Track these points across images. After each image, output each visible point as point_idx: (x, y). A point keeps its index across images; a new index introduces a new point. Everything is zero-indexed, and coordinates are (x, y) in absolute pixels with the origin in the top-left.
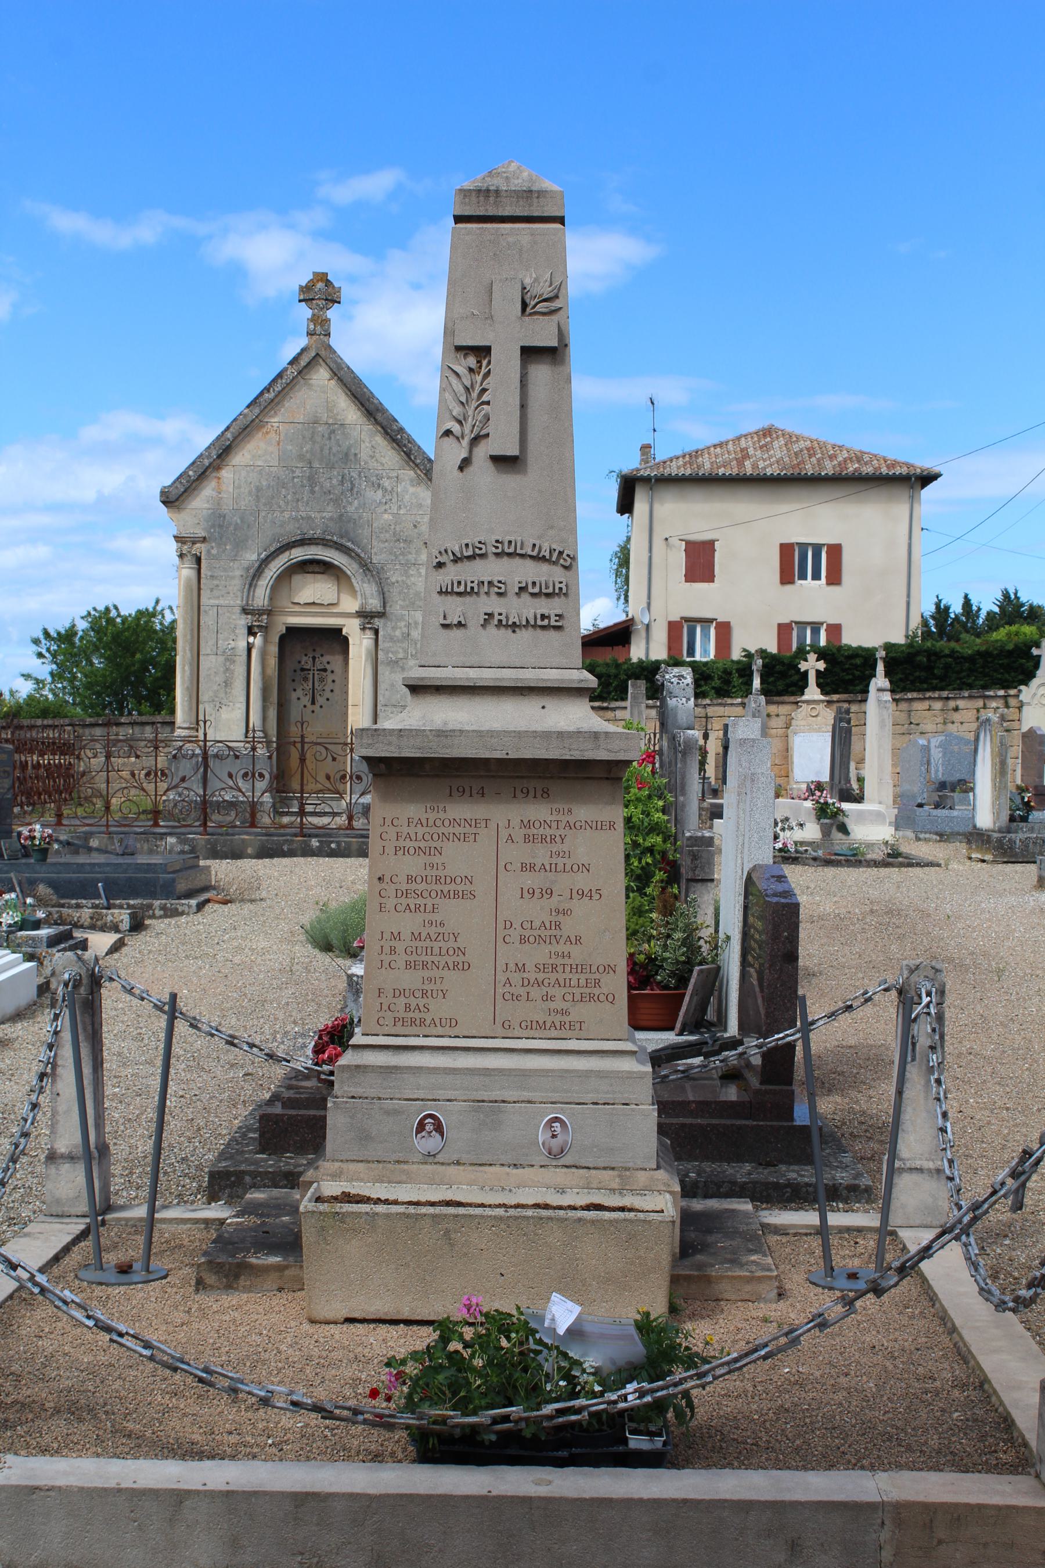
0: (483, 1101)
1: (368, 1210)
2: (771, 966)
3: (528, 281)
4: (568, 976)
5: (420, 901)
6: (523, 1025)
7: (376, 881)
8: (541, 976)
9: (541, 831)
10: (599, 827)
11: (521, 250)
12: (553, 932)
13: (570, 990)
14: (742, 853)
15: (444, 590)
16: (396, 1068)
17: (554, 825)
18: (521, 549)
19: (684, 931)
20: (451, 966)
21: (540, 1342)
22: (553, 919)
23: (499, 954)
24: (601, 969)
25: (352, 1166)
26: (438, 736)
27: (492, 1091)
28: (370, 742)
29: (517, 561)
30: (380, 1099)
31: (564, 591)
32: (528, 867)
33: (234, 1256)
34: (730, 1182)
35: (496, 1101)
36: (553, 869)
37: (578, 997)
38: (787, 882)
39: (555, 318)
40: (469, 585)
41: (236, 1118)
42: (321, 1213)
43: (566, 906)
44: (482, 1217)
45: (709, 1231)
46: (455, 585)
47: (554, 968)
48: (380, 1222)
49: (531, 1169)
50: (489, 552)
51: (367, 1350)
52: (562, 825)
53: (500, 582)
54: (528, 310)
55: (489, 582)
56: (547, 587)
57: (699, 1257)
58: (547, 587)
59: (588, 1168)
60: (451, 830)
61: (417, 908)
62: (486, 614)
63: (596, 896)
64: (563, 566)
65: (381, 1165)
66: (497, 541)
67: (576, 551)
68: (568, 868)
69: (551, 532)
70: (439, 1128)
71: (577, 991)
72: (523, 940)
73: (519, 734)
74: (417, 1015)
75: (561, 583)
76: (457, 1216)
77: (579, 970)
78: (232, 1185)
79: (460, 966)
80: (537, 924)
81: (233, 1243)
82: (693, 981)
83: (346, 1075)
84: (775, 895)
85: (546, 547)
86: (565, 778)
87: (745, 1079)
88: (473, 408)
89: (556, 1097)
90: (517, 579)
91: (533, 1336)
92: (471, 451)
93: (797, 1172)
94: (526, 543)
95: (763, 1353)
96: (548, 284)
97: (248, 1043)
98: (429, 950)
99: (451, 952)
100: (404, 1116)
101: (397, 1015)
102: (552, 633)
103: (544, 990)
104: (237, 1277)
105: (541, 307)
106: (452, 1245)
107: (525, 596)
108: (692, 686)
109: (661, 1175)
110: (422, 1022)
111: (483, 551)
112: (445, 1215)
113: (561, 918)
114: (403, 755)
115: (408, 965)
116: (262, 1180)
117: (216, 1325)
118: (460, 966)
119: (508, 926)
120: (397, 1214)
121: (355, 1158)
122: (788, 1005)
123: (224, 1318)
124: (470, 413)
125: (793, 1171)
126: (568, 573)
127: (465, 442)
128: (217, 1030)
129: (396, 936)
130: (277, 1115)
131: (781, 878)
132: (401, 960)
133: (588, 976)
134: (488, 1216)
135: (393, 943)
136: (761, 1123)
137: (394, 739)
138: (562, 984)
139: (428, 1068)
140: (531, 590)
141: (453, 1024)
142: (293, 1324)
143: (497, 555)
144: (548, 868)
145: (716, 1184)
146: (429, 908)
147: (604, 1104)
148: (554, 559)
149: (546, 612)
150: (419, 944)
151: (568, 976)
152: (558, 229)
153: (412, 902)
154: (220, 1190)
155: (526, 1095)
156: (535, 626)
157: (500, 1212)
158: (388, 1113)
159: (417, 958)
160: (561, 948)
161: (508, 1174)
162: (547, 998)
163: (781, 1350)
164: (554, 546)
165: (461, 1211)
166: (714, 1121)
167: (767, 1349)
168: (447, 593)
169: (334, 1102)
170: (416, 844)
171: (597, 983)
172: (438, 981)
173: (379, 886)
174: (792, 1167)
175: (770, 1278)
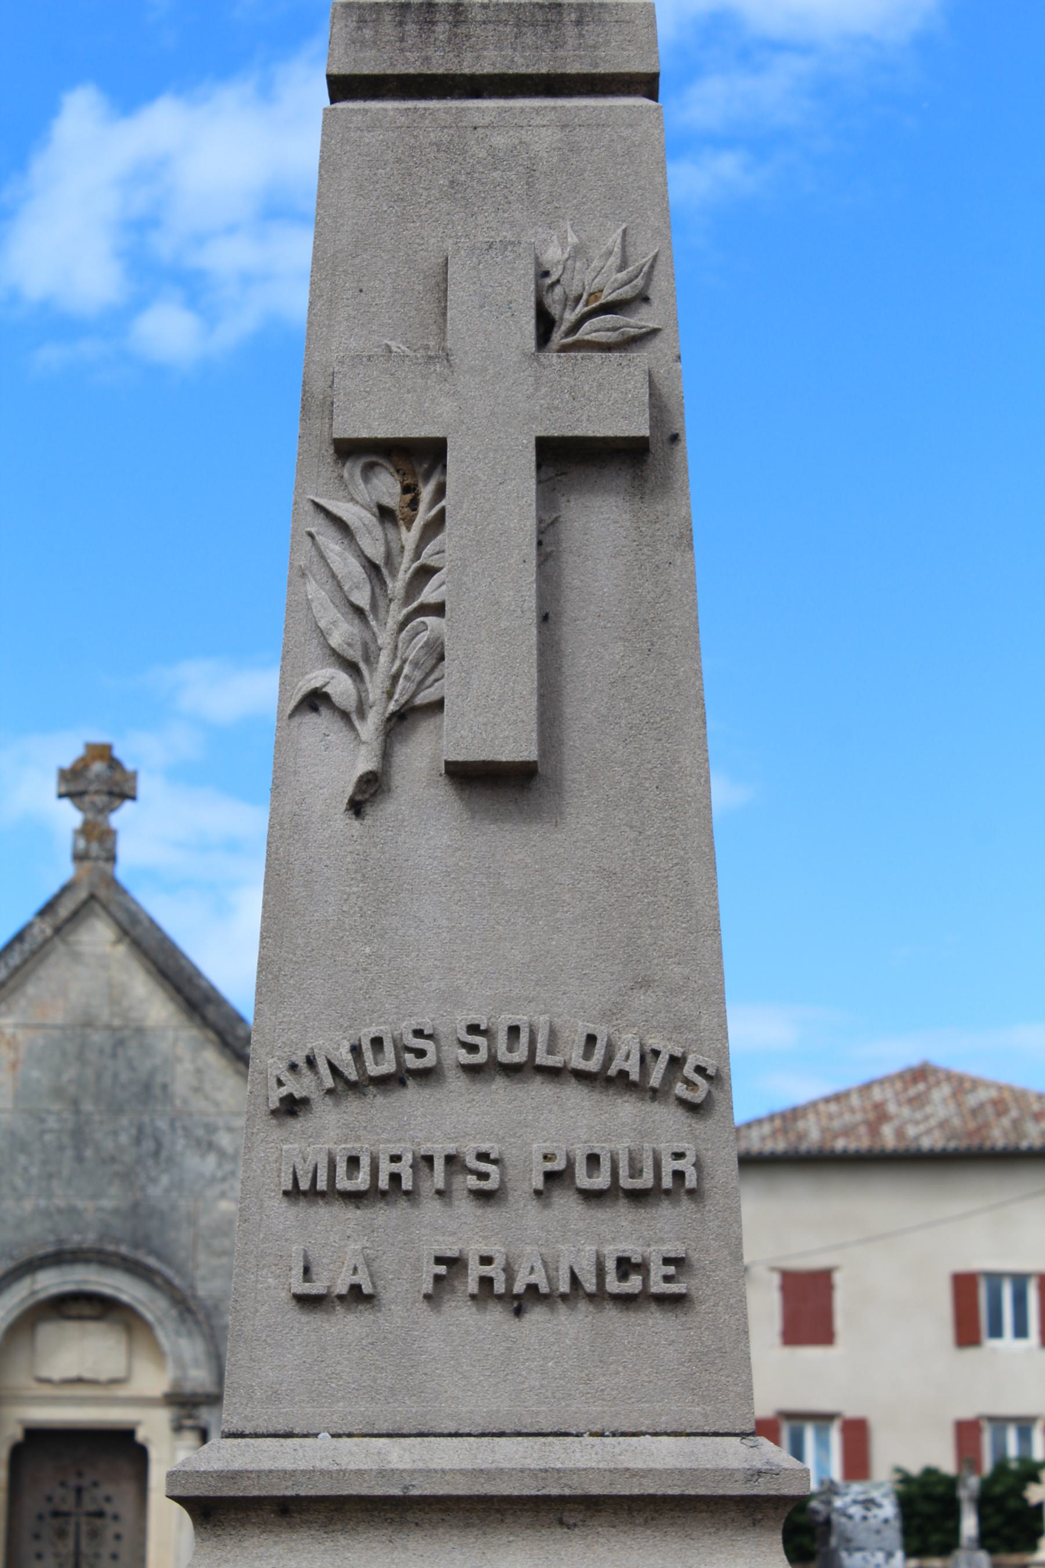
3: (553, 255)
11: (531, 170)
15: (304, 1185)
18: (550, 1051)
29: (539, 1090)
31: (691, 1182)
39: (641, 358)
40: (386, 1168)
46: (341, 1168)
50: (448, 1062)
53: (483, 1157)
54: (557, 338)
55: (451, 1160)
56: (635, 1172)
58: (635, 1172)
62: (439, 1260)
64: (683, 1102)
66: (474, 1029)
67: (723, 1053)
69: (643, 999)
75: (679, 1156)
88: (392, 624)
90: (538, 1148)
92: (386, 755)
94: (565, 1034)
96: (614, 261)
105: (593, 330)
107: (564, 1203)
108: (896, 1524)
111: (429, 1061)
124: (384, 638)
126: (699, 1127)
127: (370, 728)
140: (583, 1180)
143: (472, 1070)
148: (655, 1080)
149: (634, 1250)
152: (640, 110)
156: (600, 1297)
164: (654, 1042)
168: (314, 1194)
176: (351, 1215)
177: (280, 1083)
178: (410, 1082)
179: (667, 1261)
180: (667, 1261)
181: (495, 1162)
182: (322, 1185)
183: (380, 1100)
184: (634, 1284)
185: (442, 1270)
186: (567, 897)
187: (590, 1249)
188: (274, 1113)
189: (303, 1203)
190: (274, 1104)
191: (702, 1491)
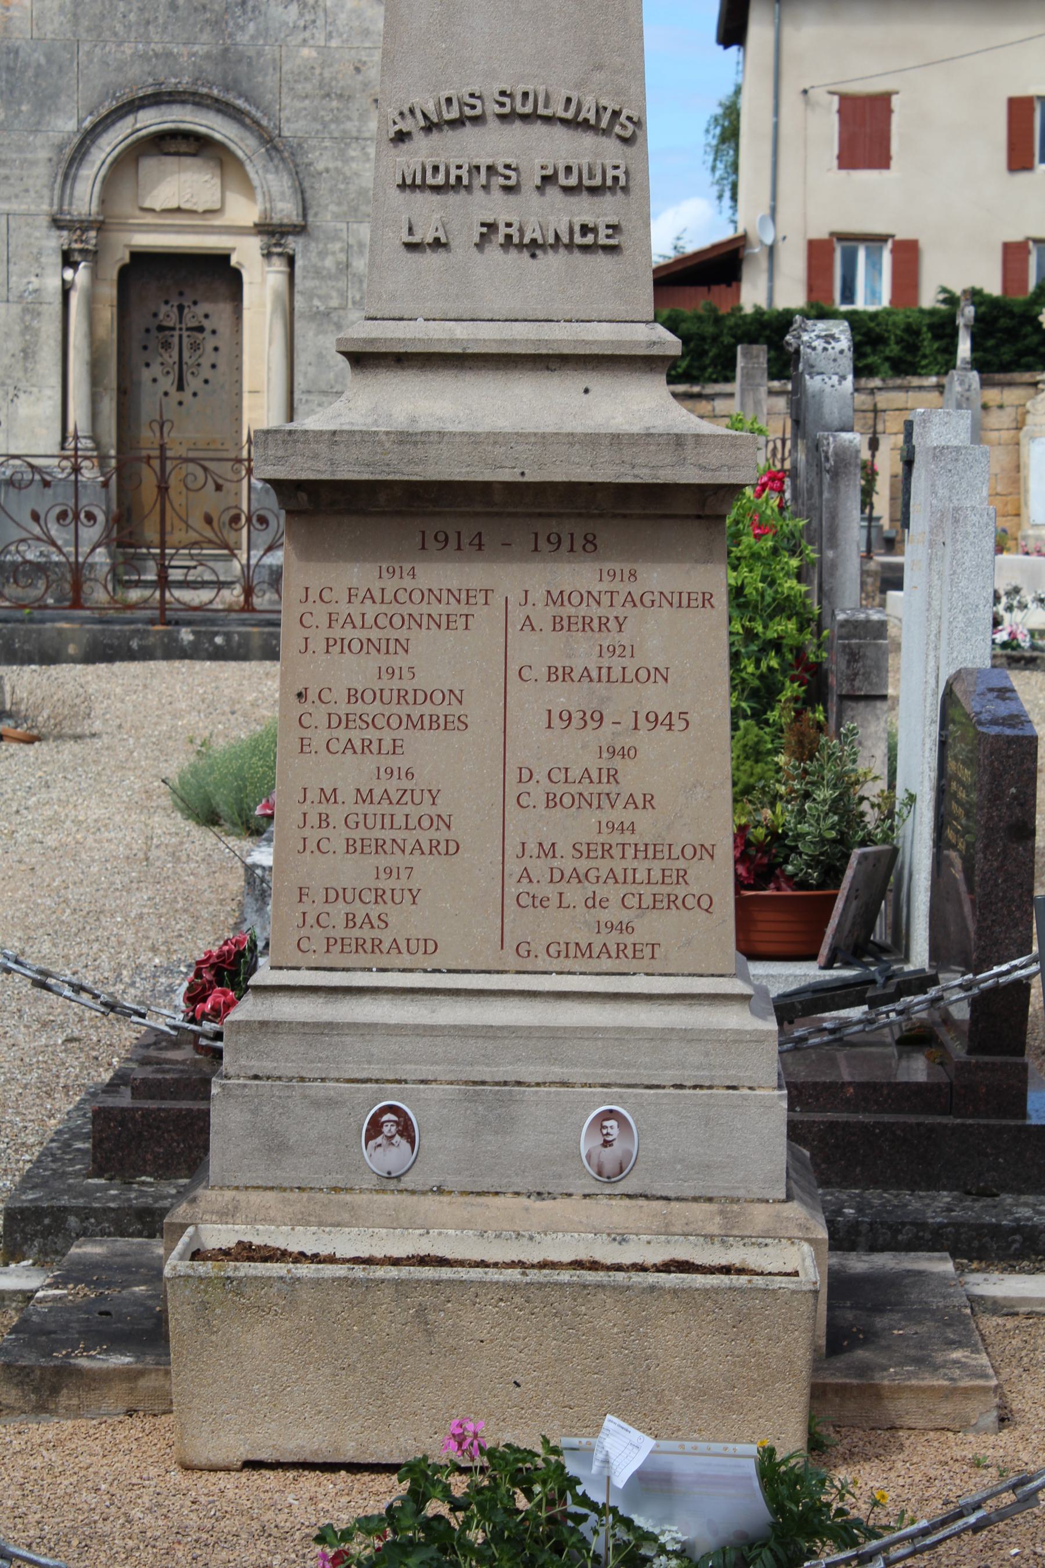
0: (483, 1083)
1: (283, 1272)
2: (986, 847)
4: (630, 863)
5: (371, 734)
6: (552, 950)
7: (293, 699)
8: (583, 865)
9: (583, 610)
10: (685, 602)
12: (605, 788)
13: (633, 889)
14: (936, 648)
15: (409, 181)
16: (330, 1025)
17: (606, 599)
18: (546, 106)
19: (835, 787)
20: (426, 848)
21: (584, 1500)
22: (604, 764)
23: (510, 827)
24: (689, 852)
25: (255, 1197)
26: (401, 443)
27: (498, 1065)
28: (280, 453)
29: (539, 128)
30: (302, 1079)
31: (622, 182)
32: (561, 674)
33: (49, 1355)
34: (912, 1224)
35: (505, 1083)
36: (604, 678)
37: (648, 901)
38: (1017, 699)
41: (51, 1116)
42: (201, 1279)
43: (628, 742)
44: (482, 1283)
45: (879, 1309)
47: (606, 851)
48: (304, 1294)
49: (568, 1200)
50: (488, 112)
51: (282, 1517)
52: (619, 600)
53: (507, 167)
56: (591, 176)
57: (861, 1354)
58: (591, 176)
59: (667, 1199)
60: (425, 609)
61: (366, 746)
62: (483, 225)
63: (680, 725)
65: (305, 1195)
66: (503, 93)
67: (643, 109)
68: (630, 675)
69: (599, 77)
70: (406, 1130)
71: (647, 891)
72: (552, 801)
73: (543, 439)
74: (366, 933)
75: (616, 167)
76: (438, 1282)
77: (650, 854)
78: (46, 1232)
79: (442, 848)
80: (575, 773)
81: (50, 1332)
82: (849, 873)
83: (243, 1039)
84: (994, 722)
85: (589, 104)
86: (624, 516)
87: (942, 1045)
89: (610, 1075)
90: (538, 162)
91: (572, 1489)
93: (1033, 1207)
94: (554, 97)
95: (972, 1519)
97: (71, 984)
98: (388, 820)
99: (425, 823)
100: (346, 1110)
101: (332, 933)
102: (601, 259)
103: (590, 889)
104: (55, 1391)
106: (429, 1333)
107: (552, 192)
108: (849, 354)
109: (795, 1210)
110: (376, 945)
111: (478, 112)
112: (418, 1281)
113: (618, 762)
114: (339, 476)
115: (350, 846)
116: (99, 1223)
117: (18, 1475)
118: (442, 848)
119: (525, 777)
120: (334, 1280)
121: (260, 1183)
122: (1018, 915)
123: (33, 1463)
125: (1026, 1205)
126: (629, 151)
128: (17, 962)
129: (330, 796)
130: (123, 1110)
131: (1005, 693)
132: (338, 836)
133: (665, 864)
134: (491, 1283)
135: (323, 808)
136: (970, 1121)
137: (323, 449)
138: (621, 879)
139: (387, 1026)
140: (562, 181)
141: (431, 947)
142: (153, 1471)
143: (502, 117)
144: (594, 674)
145: (890, 1227)
146: (387, 745)
147: (695, 1087)
148: (604, 124)
149: (589, 220)
150: (369, 809)
151: (630, 863)
153: (356, 737)
154: (25, 1240)
155: (558, 1072)
156: (570, 246)
157: (513, 1275)
158: (316, 1104)
159: (367, 834)
160: (618, 815)
161: (527, 1209)
162: (594, 902)
163: (1002, 1515)
164: (603, 102)
165: (445, 1273)
166: (887, 1118)
167: (979, 1514)
168: (413, 187)
169: (223, 1086)
170: (363, 635)
171: (682, 876)
172: (404, 874)
173: (298, 708)
174: (1024, 1198)
175: (985, 1390)
176: (435, 198)
177: (395, 123)
178: (467, 123)
179: (608, 227)
180: (608, 227)
181: (514, 170)
182: (418, 181)
183: (450, 133)
184: (590, 239)
185: (484, 230)
186: (556, 16)
187: (565, 220)
188: (392, 140)
189: (408, 191)
190: (392, 135)
191: (623, 353)
